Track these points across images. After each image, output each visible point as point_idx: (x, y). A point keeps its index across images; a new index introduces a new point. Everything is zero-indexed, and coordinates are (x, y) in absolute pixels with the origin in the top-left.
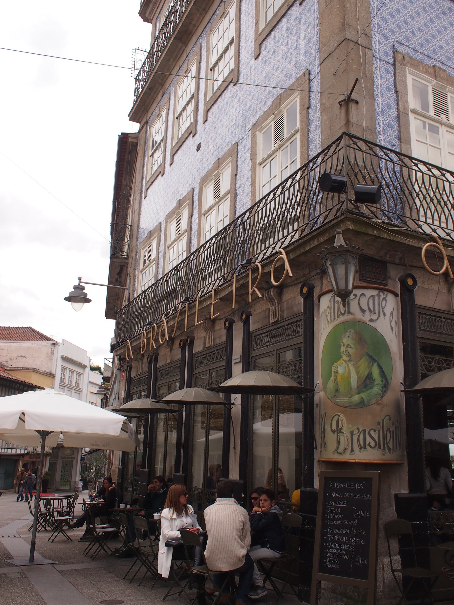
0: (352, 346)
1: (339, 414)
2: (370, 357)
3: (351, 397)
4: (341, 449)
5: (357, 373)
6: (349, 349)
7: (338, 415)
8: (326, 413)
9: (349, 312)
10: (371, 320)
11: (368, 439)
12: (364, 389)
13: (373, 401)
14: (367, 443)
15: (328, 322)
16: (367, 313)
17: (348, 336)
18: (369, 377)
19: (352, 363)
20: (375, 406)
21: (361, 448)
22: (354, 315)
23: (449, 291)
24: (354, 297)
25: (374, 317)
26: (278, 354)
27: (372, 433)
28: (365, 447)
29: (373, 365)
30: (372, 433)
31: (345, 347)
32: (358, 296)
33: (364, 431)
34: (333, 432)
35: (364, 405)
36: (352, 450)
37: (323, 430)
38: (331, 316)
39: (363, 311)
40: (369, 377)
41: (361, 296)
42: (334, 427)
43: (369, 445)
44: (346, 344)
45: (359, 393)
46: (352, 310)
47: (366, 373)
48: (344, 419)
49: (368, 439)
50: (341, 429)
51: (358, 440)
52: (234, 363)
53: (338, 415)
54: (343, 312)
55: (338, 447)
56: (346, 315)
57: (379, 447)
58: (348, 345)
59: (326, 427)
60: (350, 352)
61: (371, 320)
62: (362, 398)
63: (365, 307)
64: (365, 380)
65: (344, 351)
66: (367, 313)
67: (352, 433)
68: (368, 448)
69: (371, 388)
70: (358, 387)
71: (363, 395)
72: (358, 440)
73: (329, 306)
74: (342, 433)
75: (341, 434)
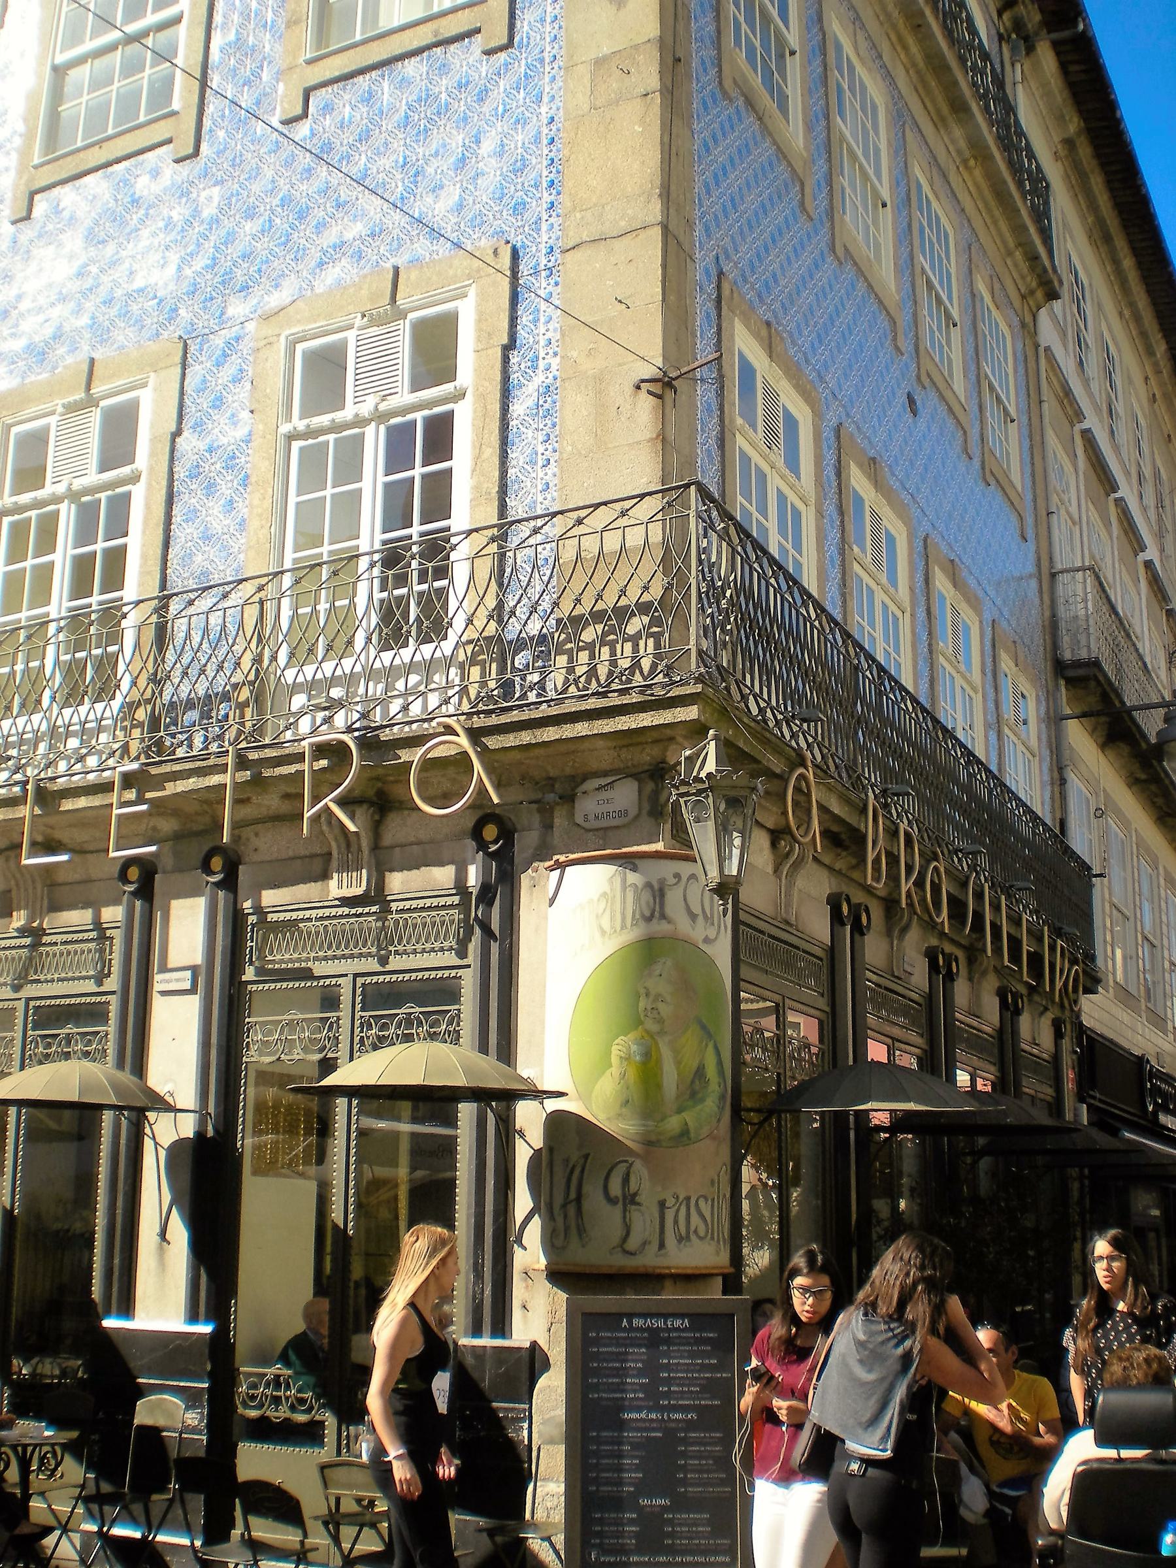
0: (668, 998)
1: (631, 1160)
2: (703, 1027)
3: (662, 1120)
4: (633, 1243)
5: (678, 1063)
6: (662, 1007)
7: (626, 1161)
8: (586, 1157)
9: (663, 916)
10: (707, 940)
11: (695, 1220)
12: (690, 1103)
13: (705, 1131)
14: (693, 1228)
15: (603, 932)
16: (700, 919)
17: (658, 972)
18: (700, 1072)
19: (667, 1039)
20: (708, 1141)
21: (680, 1239)
22: (675, 924)
23: (775, 872)
24: (675, 881)
25: (712, 933)
26: (359, 985)
27: (702, 1203)
28: (688, 1238)
29: (707, 1045)
30: (702, 1203)
31: (651, 998)
32: (684, 879)
33: (688, 1199)
34: (612, 1201)
35: (689, 1139)
36: (662, 1245)
37: (573, 1195)
38: (612, 919)
39: (693, 917)
40: (700, 1072)
41: (688, 880)
42: (615, 1189)
43: (696, 1232)
44: (653, 993)
45: (680, 1111)
46: (668, 911)
47: (695, 1065)
48: (645, 1173)
49: (695, 1220)
50: (635, 1194)
51: (676, 1222)
52: (164, 993)
53: (626, 1161)
54: (647, 913)
55: (625, 1239)
56: (655, 921)
57: (712, 1238)
58: (658, 996)
59: (586, 1189)
60: (663, 1014)
61: (707, 940)
62: (686, 1124)
63: (697, 910)
64: (693, 1082)
65: (649, 1008)
66: (700, 919)
67: (662, 1204)
68: (693, 1237)
69: (702, 1100)
70: (678, 1097)
71: (688, 1116)
72: (676, 1222)
73: (605, 894)
74: (639, 1204)
75: (633, 1207)
